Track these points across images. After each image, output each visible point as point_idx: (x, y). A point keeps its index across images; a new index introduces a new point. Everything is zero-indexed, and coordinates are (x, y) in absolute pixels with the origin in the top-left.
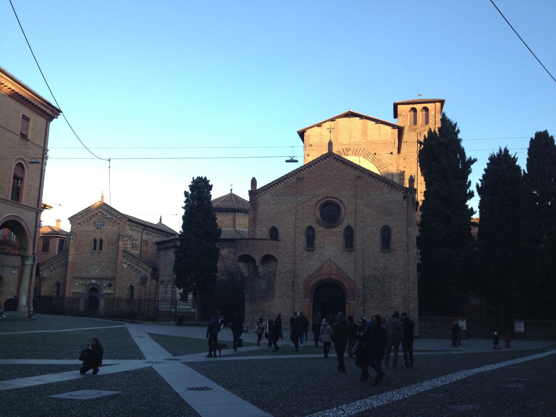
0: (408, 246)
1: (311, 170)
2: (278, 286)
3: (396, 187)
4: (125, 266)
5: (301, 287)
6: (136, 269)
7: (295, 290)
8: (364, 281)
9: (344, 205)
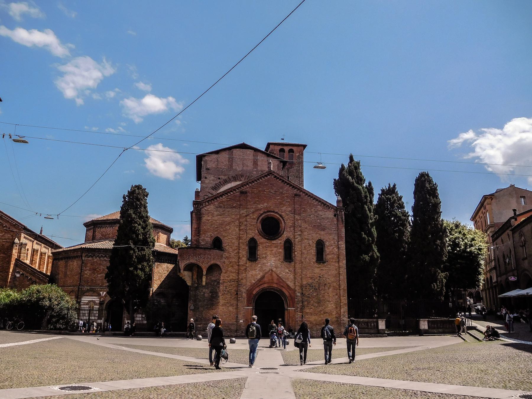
0: (338, 258)
1: (253, 185)
2: (221, 294)
3: (328, 206)
4: (18, 275)
5: (244, 295)
6: (31, 279)
7: (238, 298)
8: (302, 289)
9: (284, 220)
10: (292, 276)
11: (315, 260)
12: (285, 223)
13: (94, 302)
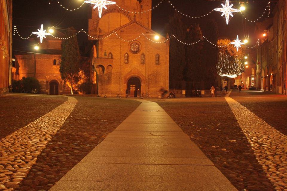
5: (123, 79)
8: (149, 77)
11: (155, 63)
12: (141, 46)
13: (43, 81)
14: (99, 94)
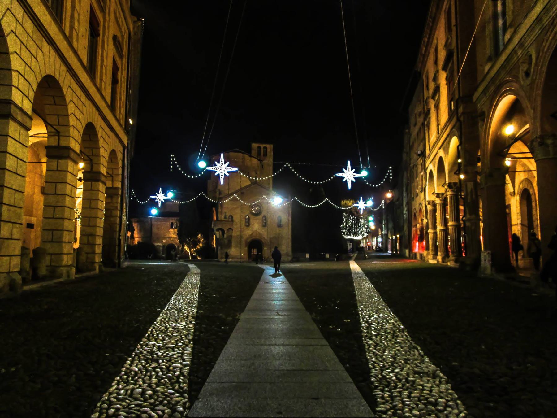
10: (266, 233)
14: (219, 259)
